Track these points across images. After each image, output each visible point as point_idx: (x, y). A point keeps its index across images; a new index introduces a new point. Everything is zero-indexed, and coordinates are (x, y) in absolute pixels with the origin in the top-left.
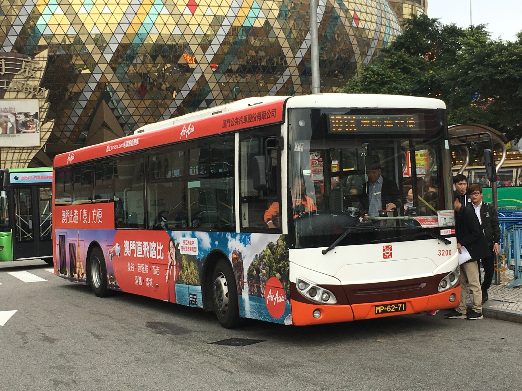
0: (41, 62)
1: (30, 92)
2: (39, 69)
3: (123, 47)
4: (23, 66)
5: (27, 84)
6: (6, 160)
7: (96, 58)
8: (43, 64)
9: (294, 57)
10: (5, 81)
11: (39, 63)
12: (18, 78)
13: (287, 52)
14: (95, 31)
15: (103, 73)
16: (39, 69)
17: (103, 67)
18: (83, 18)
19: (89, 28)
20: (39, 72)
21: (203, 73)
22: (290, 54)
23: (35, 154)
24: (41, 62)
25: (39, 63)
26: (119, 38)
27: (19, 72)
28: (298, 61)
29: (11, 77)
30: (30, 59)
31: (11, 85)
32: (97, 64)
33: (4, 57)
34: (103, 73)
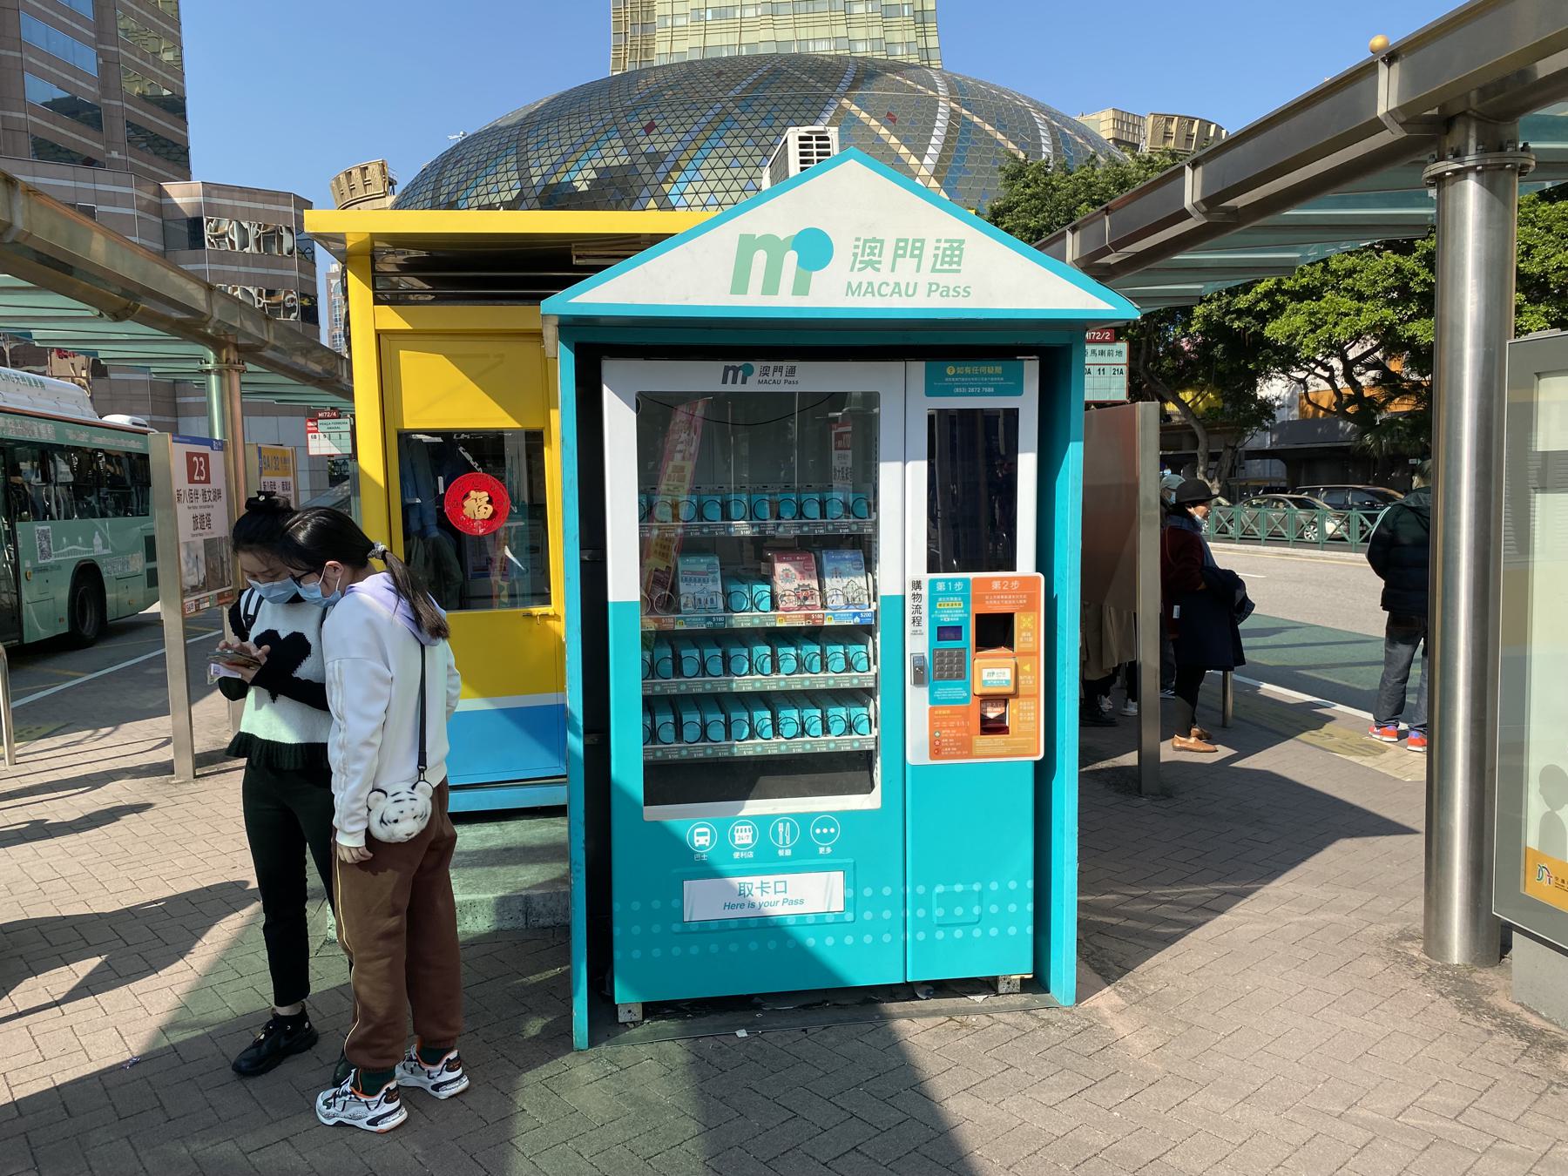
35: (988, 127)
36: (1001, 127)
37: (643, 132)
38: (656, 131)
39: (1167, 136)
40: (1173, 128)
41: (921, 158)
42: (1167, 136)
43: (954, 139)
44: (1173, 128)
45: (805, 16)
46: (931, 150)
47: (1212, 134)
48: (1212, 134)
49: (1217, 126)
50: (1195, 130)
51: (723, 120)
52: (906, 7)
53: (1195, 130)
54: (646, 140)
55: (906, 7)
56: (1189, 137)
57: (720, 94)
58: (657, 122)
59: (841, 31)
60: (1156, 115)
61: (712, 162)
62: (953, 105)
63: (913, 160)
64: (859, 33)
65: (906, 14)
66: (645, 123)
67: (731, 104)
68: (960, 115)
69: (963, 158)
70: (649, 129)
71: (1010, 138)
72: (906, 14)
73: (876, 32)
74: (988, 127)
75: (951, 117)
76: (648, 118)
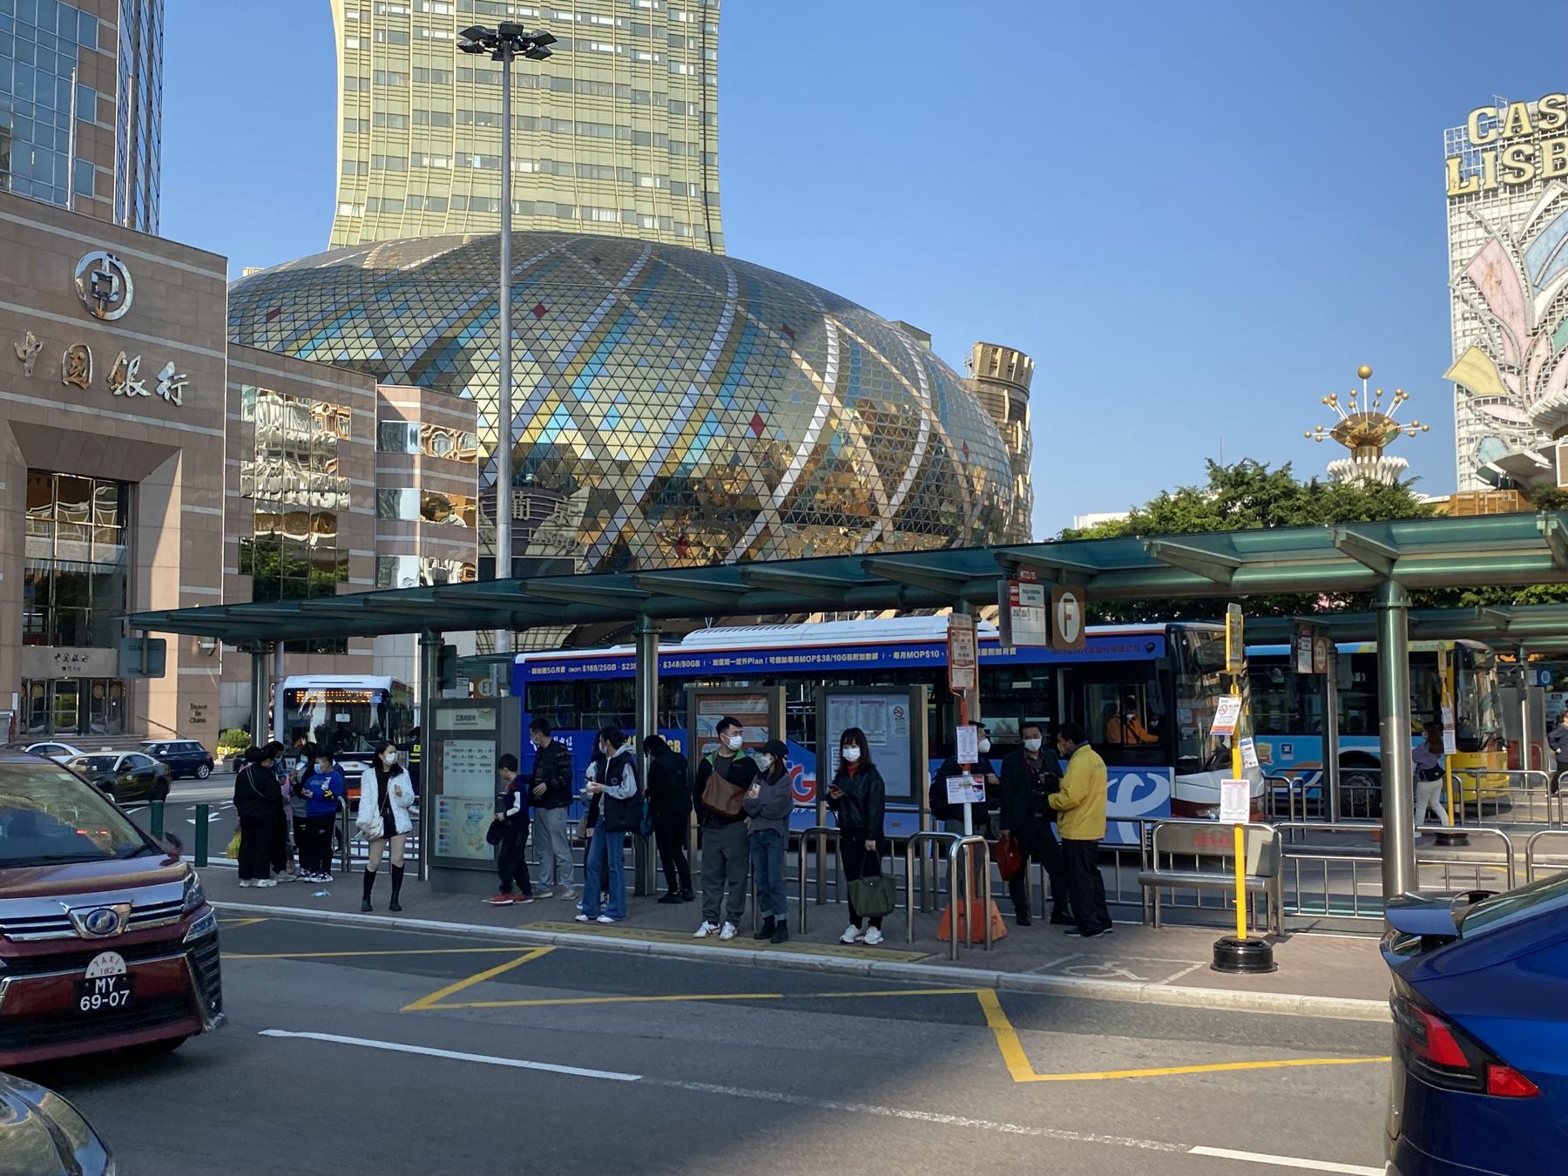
0: (580, 504)
1: (564, 547)
2: (577, 514)
3: (660, 481)
4: (556, 510)
5: (562, 536)
6: (525, 645)
7: (621, 495)
8: (583, 507)
9: (889, 504)
10: (531, 529)
11: (577, 506)
12: (546, 526)
13: (882, 499)
14: (622, 457)
15: (629, 518)
16: (577, 514)
17: (629, 509)
18: (604, 436)
19: (613, 451)
20: (576, 518)
21: (767, 523)
22: (884, 500)
23: (565, 636)
24: (580, 504)
25: (577, 506)
26: (656, 467)
27: (548, 518)
28: (894, 510)
29: (536, 523)
30: (566, 499)
31: (536, 536)
32: (621, 504)
33: (530, 495)
34: (629, 518)
35: (872, 350)
36: (882, 351)
37: (533, 315)
38: (546, 316)
39: (993, 366)
40: (998, 357)
41: (822, 375)
42: (993, 366)
43: (847, 358)
44: (998, 357)
45: (588, 180)
46: (829, 368)
47: (1026, 365)
48: (1026, 365)
49: (1020, 353)
50: (1014, 360)
51: (619, 314)
52: (693, 186)
53: (1014, 360)
54: (539, 325)
55: (693, 186)
56: (1011, 366)
57: (608, 284)
58: (547, 307)
59: (629, 203)
60: (985, 345)
61: (619, 358)
62: (837, 323)
63: (816, 378)
64: (646, 208)
65: (693, 194)
66: (533, 306)
67: (625, 297)
68: (845, 334)
69: (858, 379)
70: (539, 311)
71: (893, 362)
72: (693, 194)
73: (665, 210)
74: (872, 350)
75: (840, 337)
76: (533, 299)
